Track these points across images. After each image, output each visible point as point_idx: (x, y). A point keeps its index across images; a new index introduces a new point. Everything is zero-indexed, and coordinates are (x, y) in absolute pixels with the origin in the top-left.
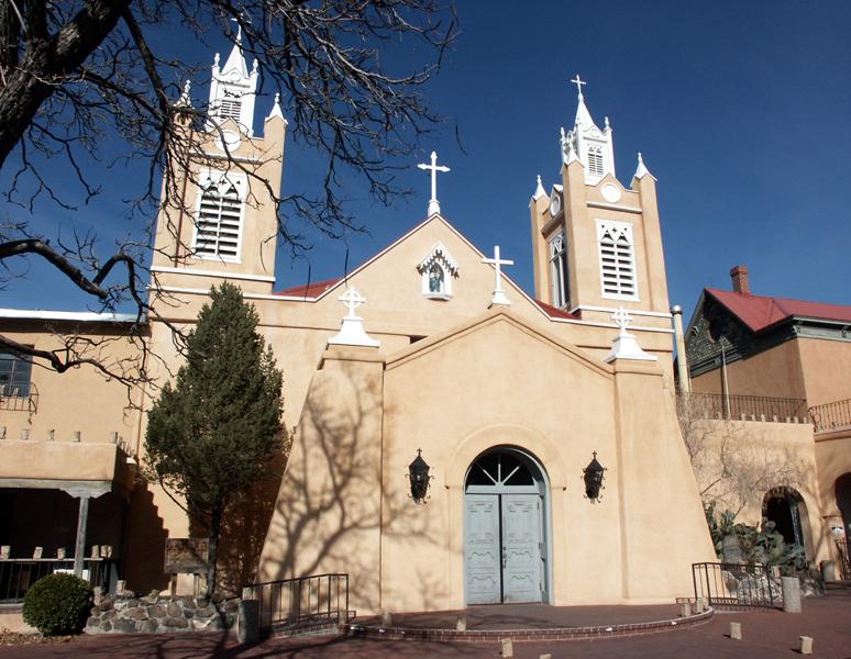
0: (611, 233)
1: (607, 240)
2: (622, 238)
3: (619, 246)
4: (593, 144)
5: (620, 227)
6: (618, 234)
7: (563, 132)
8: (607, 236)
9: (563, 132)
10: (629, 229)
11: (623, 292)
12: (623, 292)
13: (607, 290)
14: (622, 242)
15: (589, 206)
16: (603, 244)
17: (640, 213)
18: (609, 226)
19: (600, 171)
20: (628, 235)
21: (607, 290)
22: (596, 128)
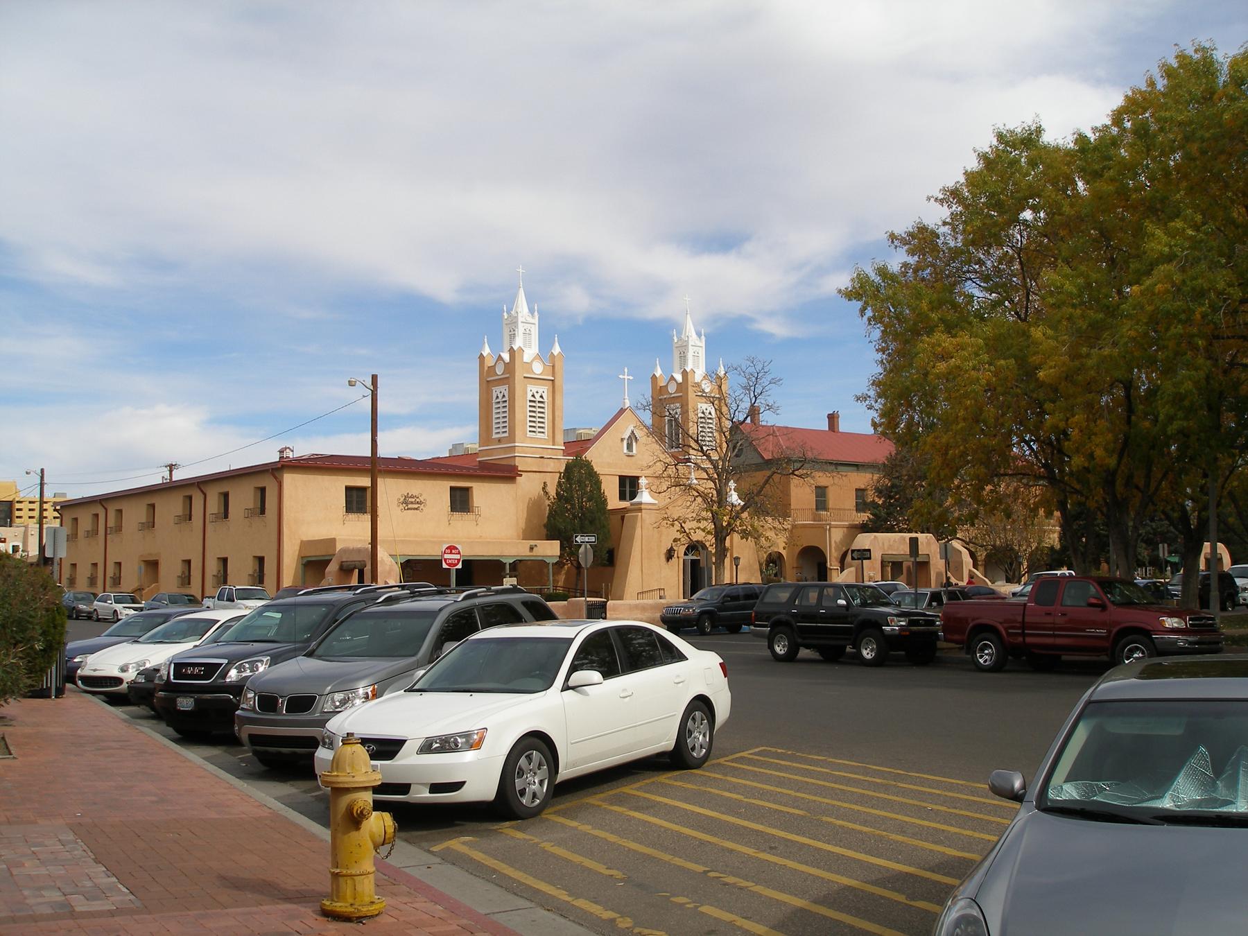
0: (535, 394)
1: (533, 399)
2: (541, 397)
3: (539, 402)
4: (527, 326)
6: (539, 394)
8: (533, 396)
10: (546, 392)
11: (540, 432)
13: (530, 431)
14: (541, 400)
15: (525, 377)
16: (530, 401)
17: (553, 380)
18: (534, 391)
20: (545, 396)
21: (530, 431)
22: (530, 315)
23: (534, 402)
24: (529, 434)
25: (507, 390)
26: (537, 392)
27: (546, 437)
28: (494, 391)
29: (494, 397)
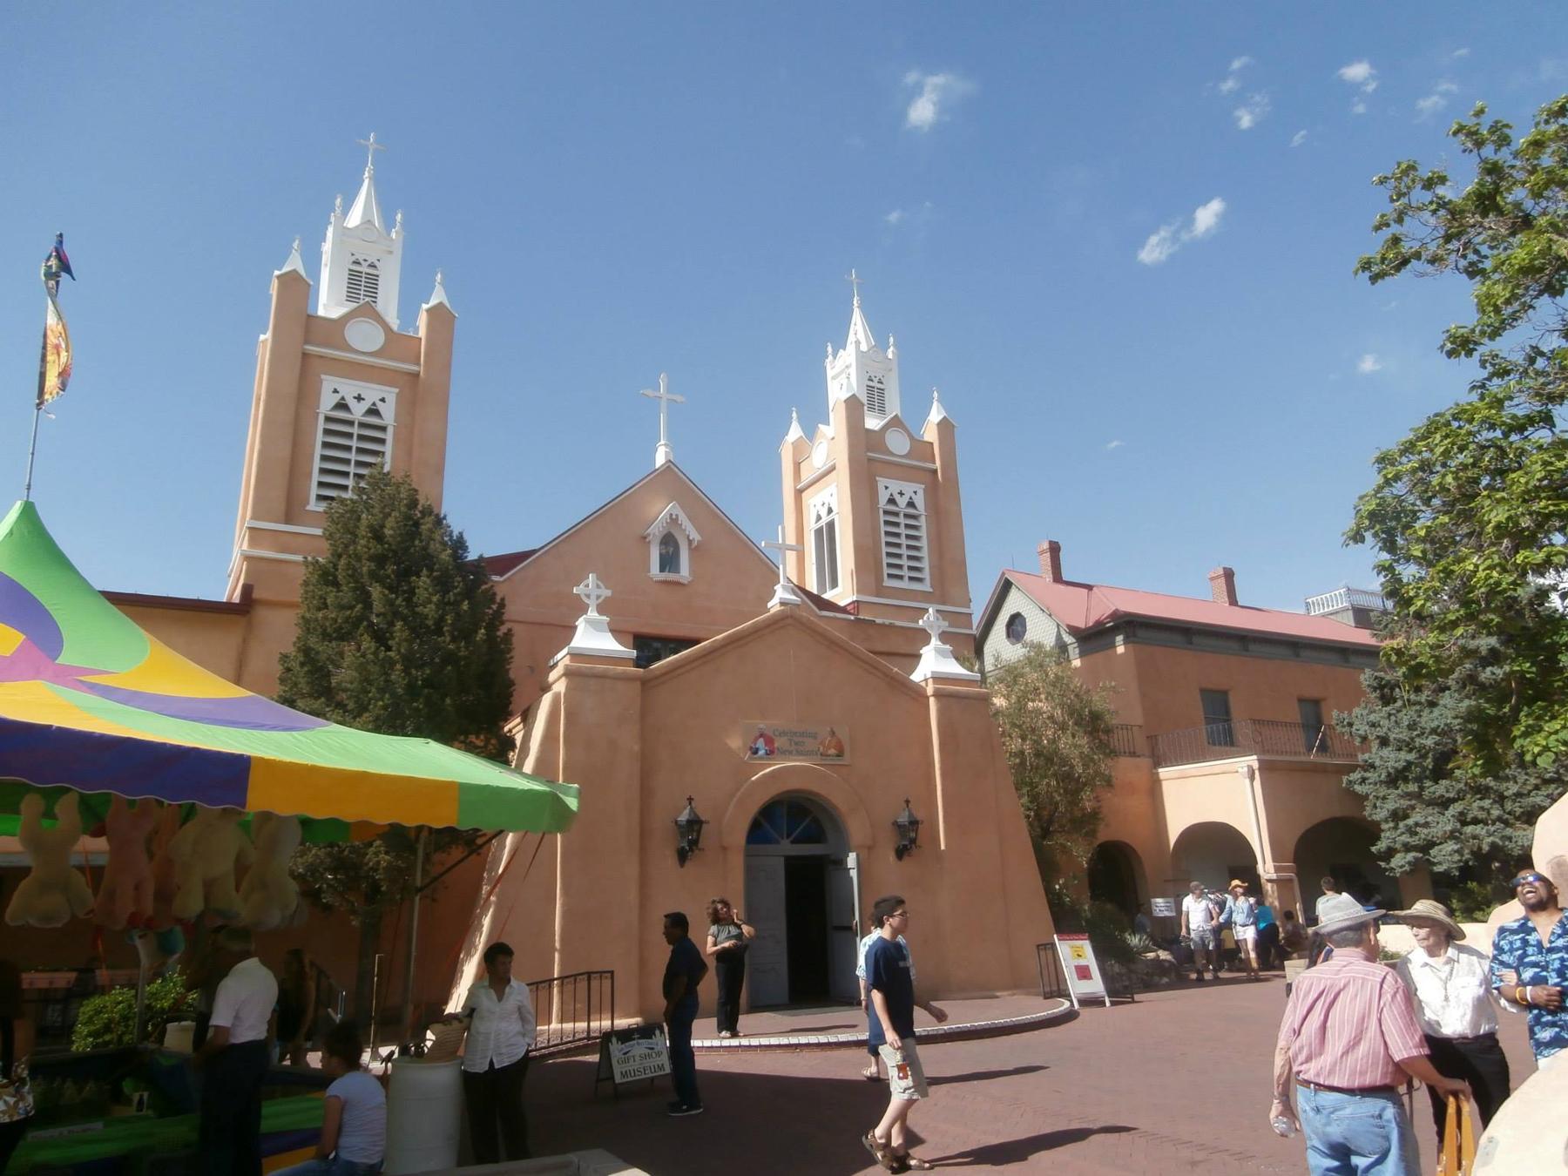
0: (897, 497)
1: (892, 508)
2: (911, 504)
3: (907, 516)
5: (908, 494)
7: (830, 349)
8: (892, 501)
9: (830, 349)
11: (911, 579)
12: (911, 579)
13: (890, 576)
14: (911, 511)
16: (886, 512)
19: (882, 410)
21: (890, 576)
23: (896, 514)
24: (888, 583)
25: (835, 496)
26: (901, 494)
27: (926, 587)
28: (812, 506)
29: (814, 518)
